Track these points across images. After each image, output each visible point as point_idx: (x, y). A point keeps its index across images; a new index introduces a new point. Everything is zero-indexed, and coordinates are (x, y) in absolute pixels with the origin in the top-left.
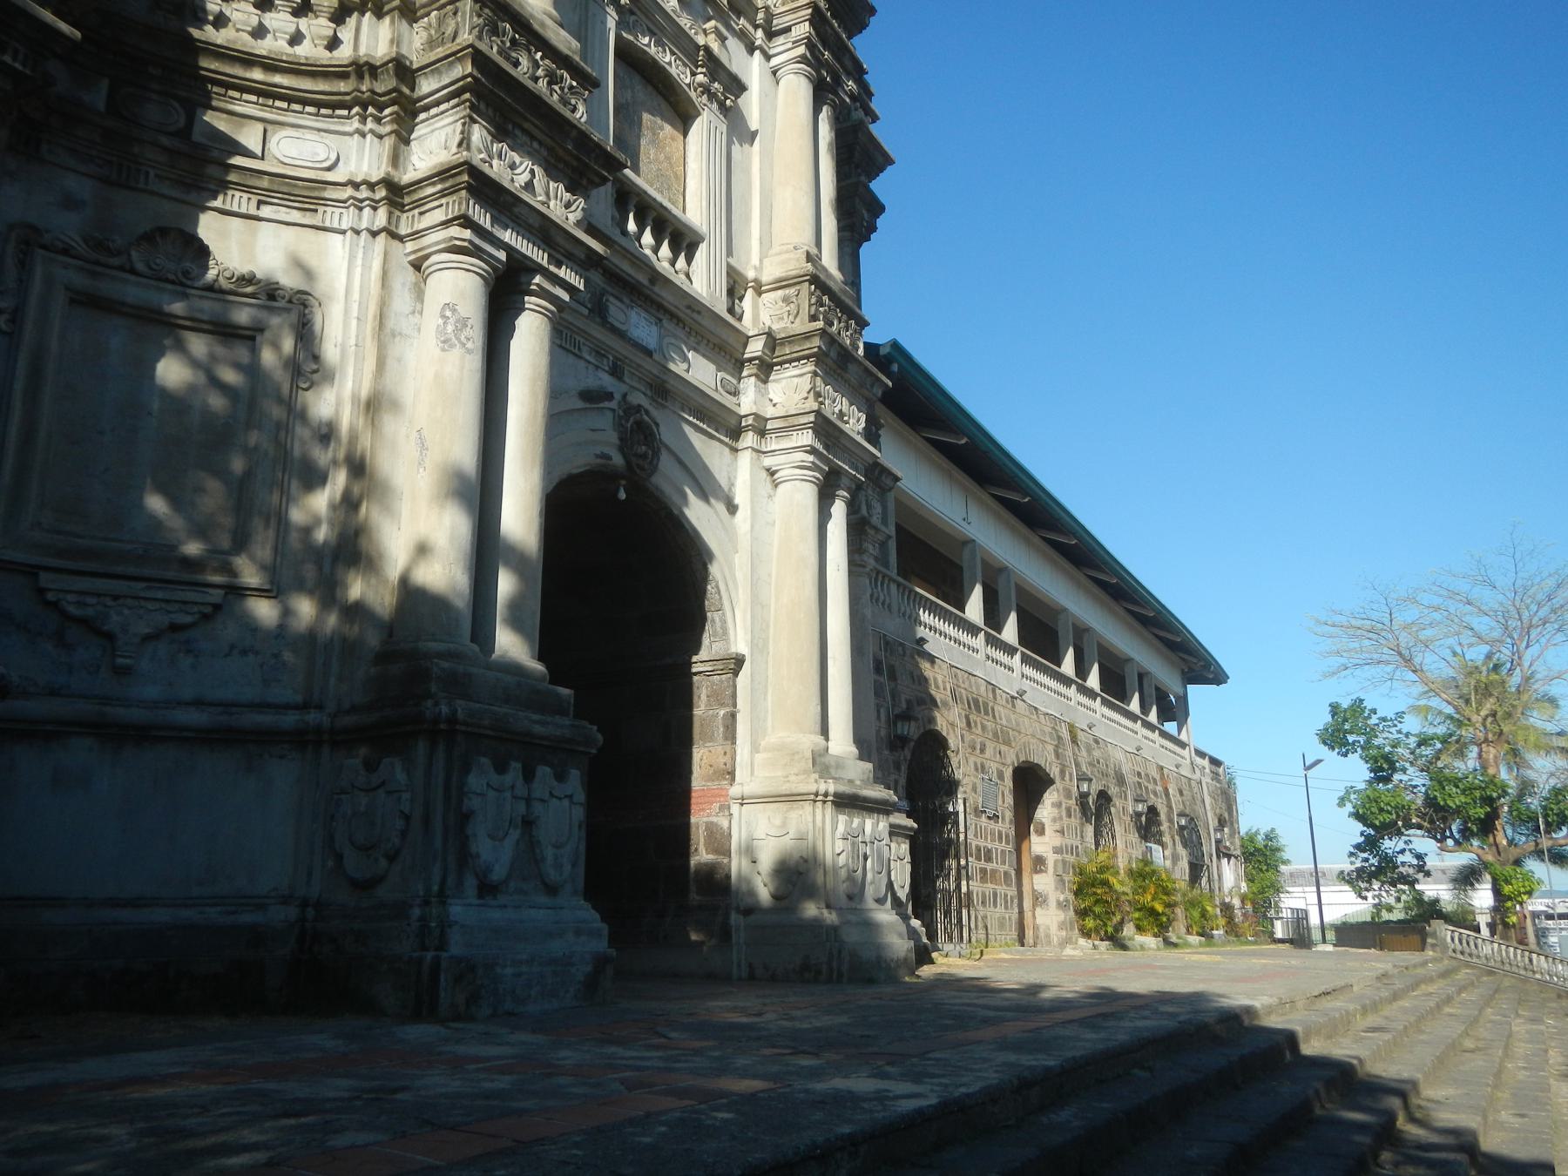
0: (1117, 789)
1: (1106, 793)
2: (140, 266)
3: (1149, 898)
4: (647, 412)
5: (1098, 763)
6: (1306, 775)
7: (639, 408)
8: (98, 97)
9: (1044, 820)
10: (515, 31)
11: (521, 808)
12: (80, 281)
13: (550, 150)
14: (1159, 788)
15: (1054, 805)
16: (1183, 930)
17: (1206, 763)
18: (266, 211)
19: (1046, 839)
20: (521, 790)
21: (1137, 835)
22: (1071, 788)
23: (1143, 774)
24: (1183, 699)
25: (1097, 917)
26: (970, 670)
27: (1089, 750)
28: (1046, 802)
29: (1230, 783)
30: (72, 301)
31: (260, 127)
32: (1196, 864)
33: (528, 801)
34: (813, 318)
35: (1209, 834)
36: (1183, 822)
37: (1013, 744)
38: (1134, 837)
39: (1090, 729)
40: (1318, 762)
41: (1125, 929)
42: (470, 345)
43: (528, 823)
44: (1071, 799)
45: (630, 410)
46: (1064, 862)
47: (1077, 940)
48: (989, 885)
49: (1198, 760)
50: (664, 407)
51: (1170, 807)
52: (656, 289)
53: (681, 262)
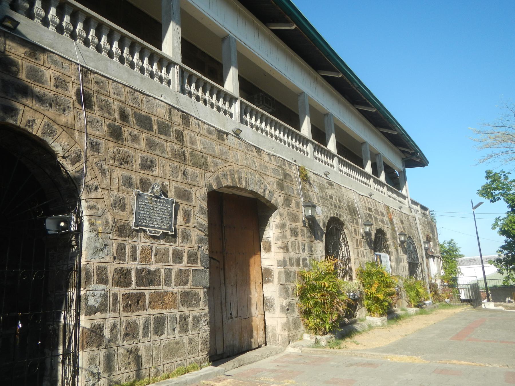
0: (349, 217)
1: (339, 220)
3: (374, 291)
5: (331, 198)
6: (474, 211)
9: (270, 239)
14: (386, 219)
15: (277, 226)
16: (405, 304)
17: (418, 208)
19: (272, 254)
21: (367, 248)
22: (297, 213)
23: (373, 209)
24: (403, 173)
25: (318, 316)
26: (136, 86)
27: (322, 188)
28: (271, 224)
29: (433, 219)
32: (414, 263)
35: (421, 245)
36: (402, 239)
37: (212, 169)
38: (366, 249)
39: (326, 175)
40: (481, 203)
41: (358, 313)
44: (298, 221)
46: (287, 274)
47: (302, 336)
48: (151, 311)
49: (413, 206)
51: (394, 230)
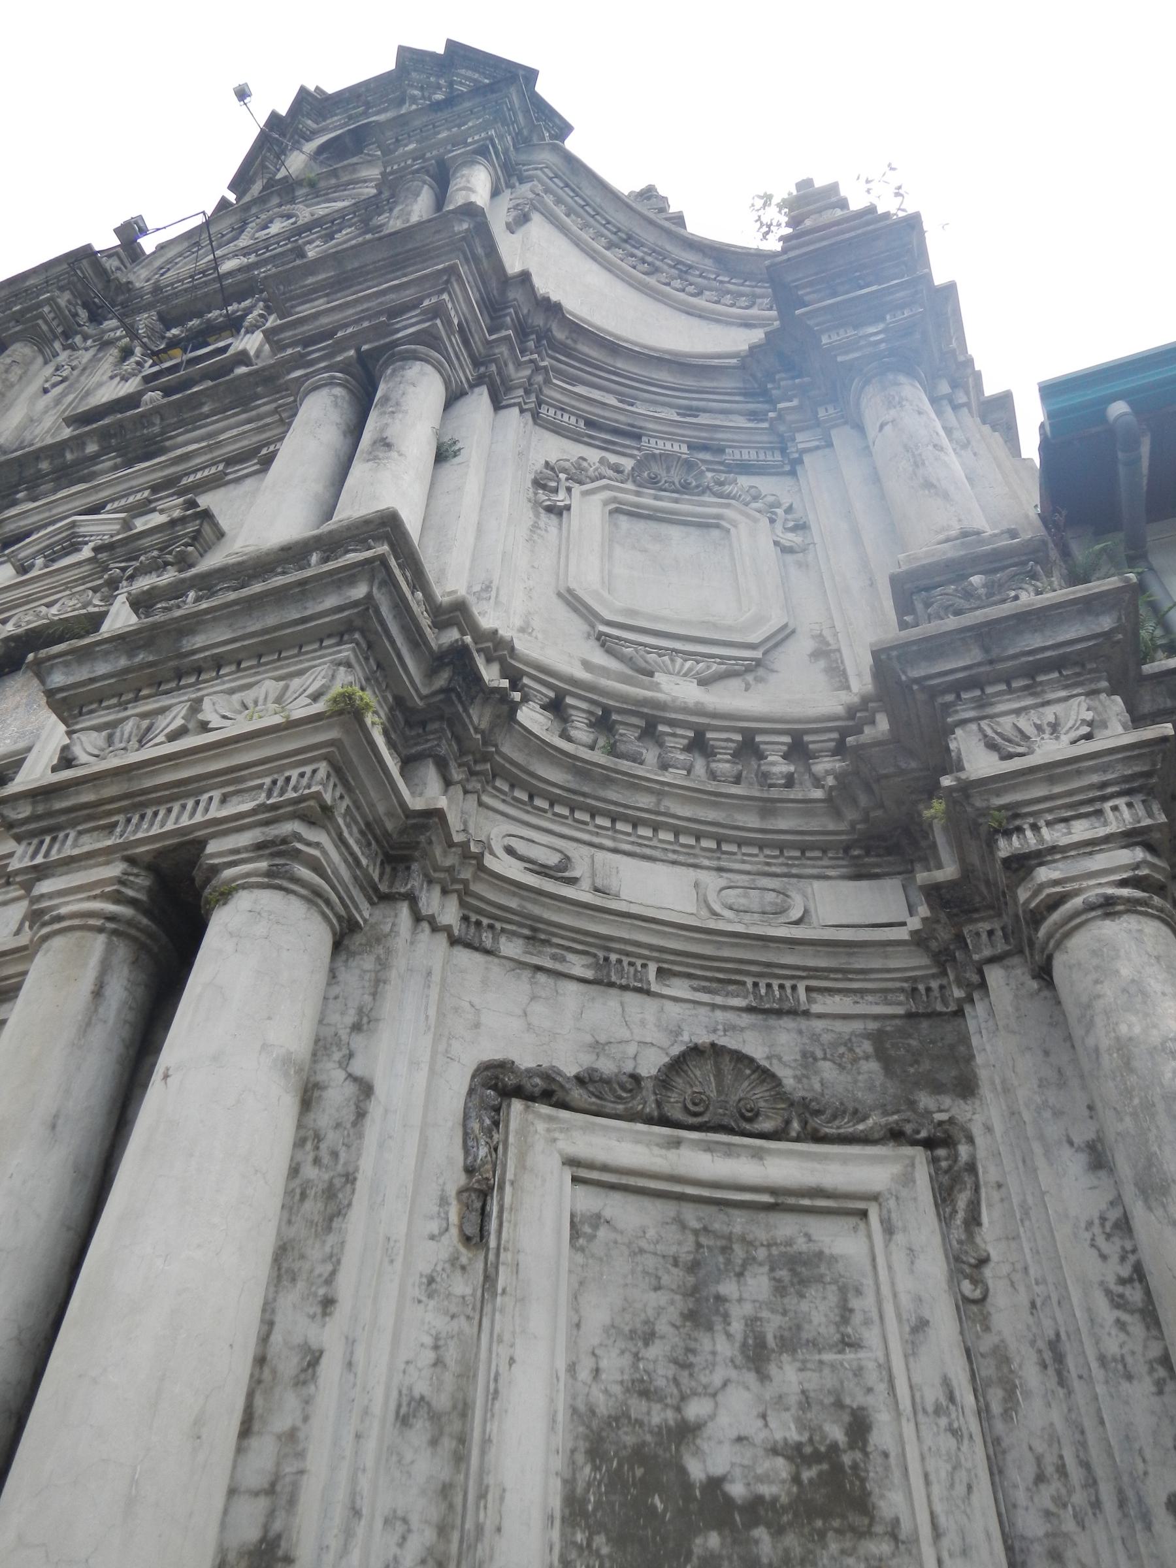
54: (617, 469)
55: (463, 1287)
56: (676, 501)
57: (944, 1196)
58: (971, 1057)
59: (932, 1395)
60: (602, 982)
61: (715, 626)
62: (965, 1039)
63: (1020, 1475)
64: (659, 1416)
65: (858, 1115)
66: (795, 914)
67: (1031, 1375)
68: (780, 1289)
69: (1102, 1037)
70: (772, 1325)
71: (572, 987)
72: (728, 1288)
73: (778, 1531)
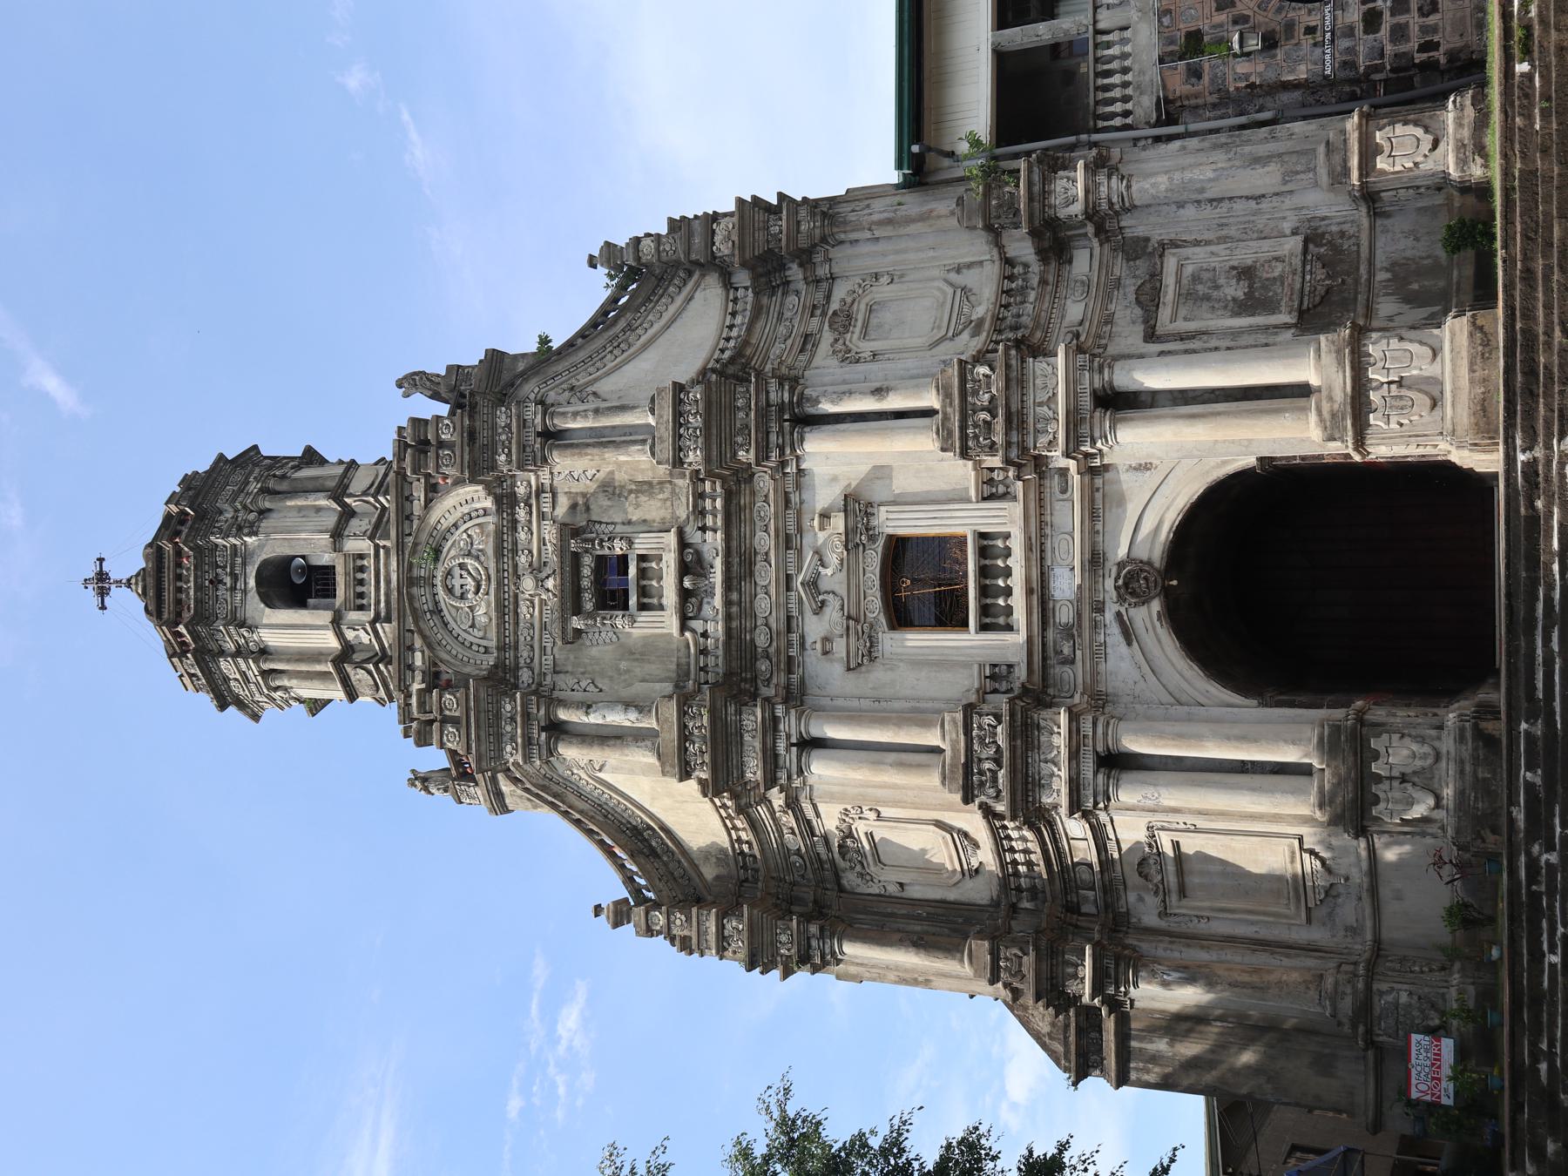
2: (1159, 877)
4: (1116, 580)
7: (1117, 588)
8: (1090, 894)
10: (972, 775)
11: (1396, 784)
12: (1174, 897)
13: (1027, 750)
18: (1112, 836)
20: (1385, 785)
30: (1185, 897)
31: (1071, 841)
33: (1391, 778)
34: (992, 447)
42: (1156, 795)
43: (1403, 779)
45: (1121, 599)
50: (1104, 554)
52: (1035, 585)
53: (1000, 543)
54: (836, 340)
55: (1205, 337)
56: (856, 320)
57: (1178, 247)
58: (1138, 237)
59: (1228, 252)
60: (1111, 322)
61: (943, 304)
62: (1132, 238)
63: (1245, 237)
64: (1231, 304)
65: (1156, 263)
66: (1085, 278)
67: (1223, 233)
68: (1201, 283)
69: (1162, 195)
70: (1209, 284)
71: (1114, 329)
72: (1201, 293)
73: (1254, 283)
